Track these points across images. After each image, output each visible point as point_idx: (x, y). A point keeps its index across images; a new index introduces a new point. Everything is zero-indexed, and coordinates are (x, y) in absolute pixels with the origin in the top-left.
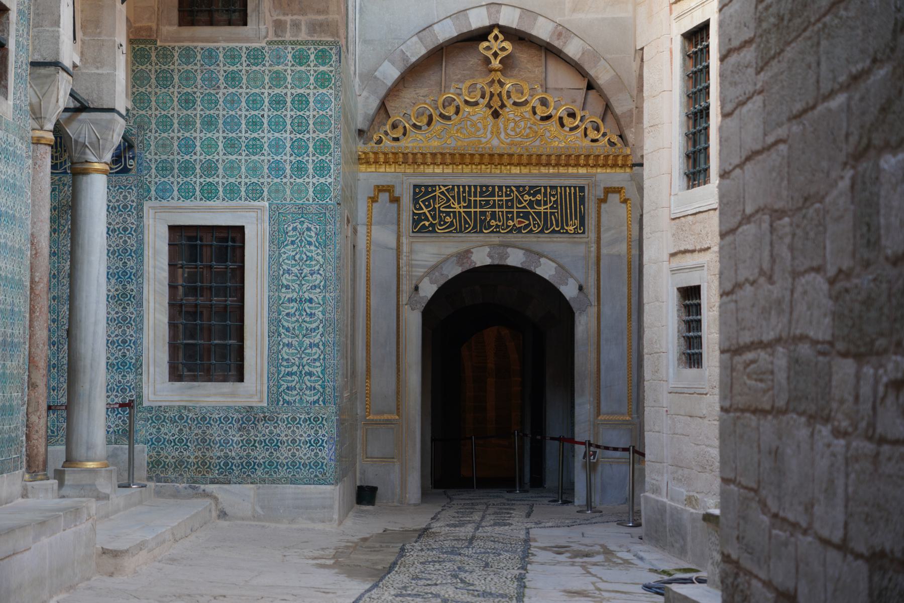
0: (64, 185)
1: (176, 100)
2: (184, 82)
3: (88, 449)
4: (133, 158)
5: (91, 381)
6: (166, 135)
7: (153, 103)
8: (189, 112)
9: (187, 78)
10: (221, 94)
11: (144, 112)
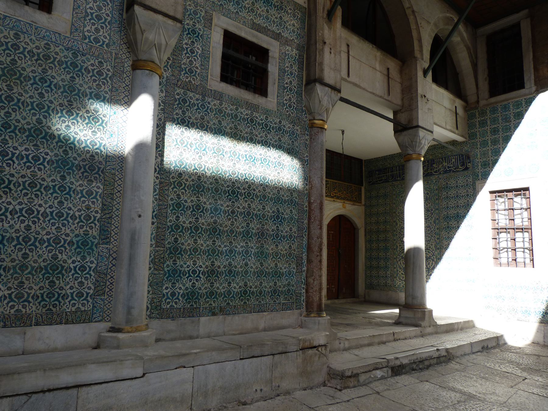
0: (440, 179)
1: (489, 132)
2: (493, 123)
3: (413, 298)
4: (470, 162)
5: (414, 263)
6: (485, 149)
7: (478, 136)
8: (496, 136)
9: (494, 120)
10: (512, 124)
11: (474, 141)
